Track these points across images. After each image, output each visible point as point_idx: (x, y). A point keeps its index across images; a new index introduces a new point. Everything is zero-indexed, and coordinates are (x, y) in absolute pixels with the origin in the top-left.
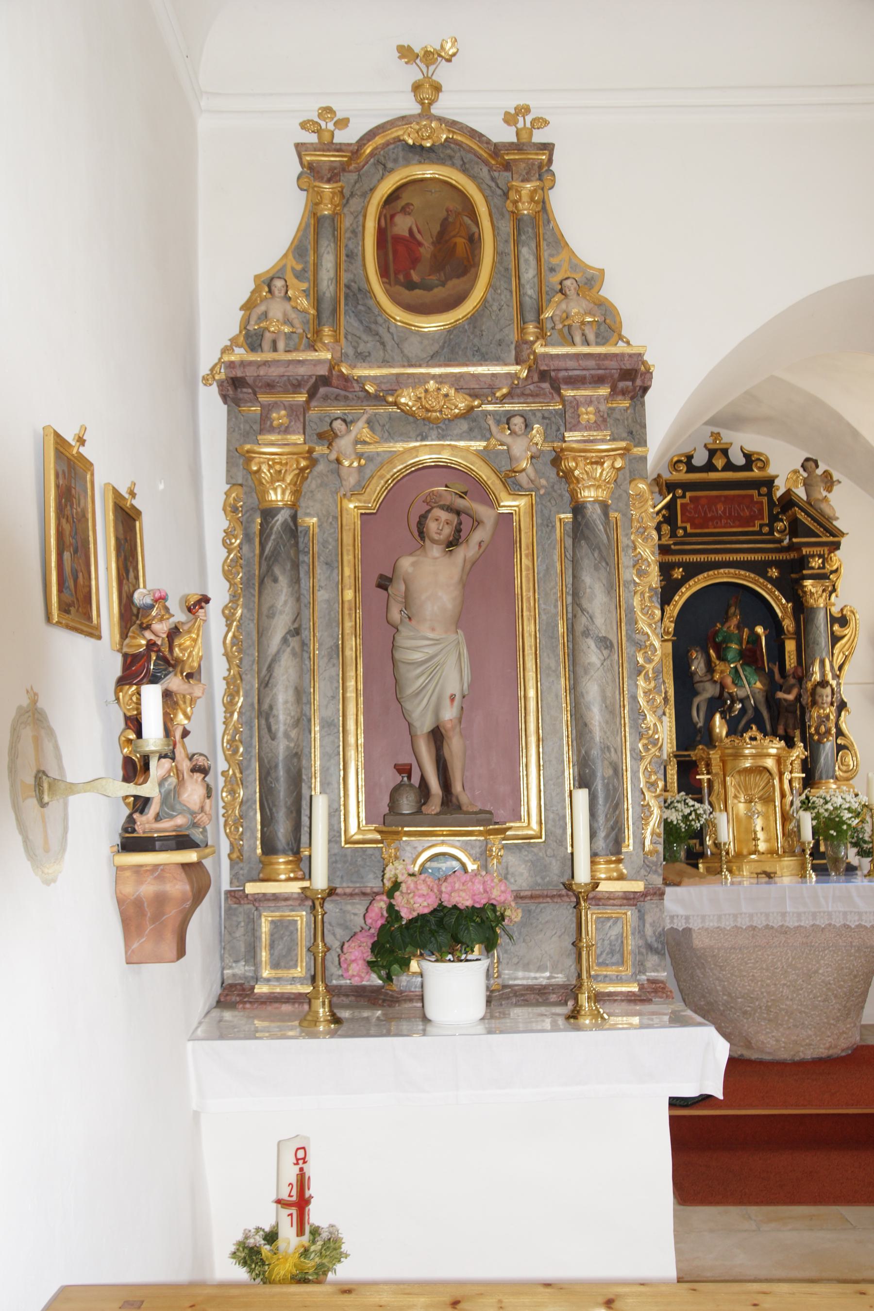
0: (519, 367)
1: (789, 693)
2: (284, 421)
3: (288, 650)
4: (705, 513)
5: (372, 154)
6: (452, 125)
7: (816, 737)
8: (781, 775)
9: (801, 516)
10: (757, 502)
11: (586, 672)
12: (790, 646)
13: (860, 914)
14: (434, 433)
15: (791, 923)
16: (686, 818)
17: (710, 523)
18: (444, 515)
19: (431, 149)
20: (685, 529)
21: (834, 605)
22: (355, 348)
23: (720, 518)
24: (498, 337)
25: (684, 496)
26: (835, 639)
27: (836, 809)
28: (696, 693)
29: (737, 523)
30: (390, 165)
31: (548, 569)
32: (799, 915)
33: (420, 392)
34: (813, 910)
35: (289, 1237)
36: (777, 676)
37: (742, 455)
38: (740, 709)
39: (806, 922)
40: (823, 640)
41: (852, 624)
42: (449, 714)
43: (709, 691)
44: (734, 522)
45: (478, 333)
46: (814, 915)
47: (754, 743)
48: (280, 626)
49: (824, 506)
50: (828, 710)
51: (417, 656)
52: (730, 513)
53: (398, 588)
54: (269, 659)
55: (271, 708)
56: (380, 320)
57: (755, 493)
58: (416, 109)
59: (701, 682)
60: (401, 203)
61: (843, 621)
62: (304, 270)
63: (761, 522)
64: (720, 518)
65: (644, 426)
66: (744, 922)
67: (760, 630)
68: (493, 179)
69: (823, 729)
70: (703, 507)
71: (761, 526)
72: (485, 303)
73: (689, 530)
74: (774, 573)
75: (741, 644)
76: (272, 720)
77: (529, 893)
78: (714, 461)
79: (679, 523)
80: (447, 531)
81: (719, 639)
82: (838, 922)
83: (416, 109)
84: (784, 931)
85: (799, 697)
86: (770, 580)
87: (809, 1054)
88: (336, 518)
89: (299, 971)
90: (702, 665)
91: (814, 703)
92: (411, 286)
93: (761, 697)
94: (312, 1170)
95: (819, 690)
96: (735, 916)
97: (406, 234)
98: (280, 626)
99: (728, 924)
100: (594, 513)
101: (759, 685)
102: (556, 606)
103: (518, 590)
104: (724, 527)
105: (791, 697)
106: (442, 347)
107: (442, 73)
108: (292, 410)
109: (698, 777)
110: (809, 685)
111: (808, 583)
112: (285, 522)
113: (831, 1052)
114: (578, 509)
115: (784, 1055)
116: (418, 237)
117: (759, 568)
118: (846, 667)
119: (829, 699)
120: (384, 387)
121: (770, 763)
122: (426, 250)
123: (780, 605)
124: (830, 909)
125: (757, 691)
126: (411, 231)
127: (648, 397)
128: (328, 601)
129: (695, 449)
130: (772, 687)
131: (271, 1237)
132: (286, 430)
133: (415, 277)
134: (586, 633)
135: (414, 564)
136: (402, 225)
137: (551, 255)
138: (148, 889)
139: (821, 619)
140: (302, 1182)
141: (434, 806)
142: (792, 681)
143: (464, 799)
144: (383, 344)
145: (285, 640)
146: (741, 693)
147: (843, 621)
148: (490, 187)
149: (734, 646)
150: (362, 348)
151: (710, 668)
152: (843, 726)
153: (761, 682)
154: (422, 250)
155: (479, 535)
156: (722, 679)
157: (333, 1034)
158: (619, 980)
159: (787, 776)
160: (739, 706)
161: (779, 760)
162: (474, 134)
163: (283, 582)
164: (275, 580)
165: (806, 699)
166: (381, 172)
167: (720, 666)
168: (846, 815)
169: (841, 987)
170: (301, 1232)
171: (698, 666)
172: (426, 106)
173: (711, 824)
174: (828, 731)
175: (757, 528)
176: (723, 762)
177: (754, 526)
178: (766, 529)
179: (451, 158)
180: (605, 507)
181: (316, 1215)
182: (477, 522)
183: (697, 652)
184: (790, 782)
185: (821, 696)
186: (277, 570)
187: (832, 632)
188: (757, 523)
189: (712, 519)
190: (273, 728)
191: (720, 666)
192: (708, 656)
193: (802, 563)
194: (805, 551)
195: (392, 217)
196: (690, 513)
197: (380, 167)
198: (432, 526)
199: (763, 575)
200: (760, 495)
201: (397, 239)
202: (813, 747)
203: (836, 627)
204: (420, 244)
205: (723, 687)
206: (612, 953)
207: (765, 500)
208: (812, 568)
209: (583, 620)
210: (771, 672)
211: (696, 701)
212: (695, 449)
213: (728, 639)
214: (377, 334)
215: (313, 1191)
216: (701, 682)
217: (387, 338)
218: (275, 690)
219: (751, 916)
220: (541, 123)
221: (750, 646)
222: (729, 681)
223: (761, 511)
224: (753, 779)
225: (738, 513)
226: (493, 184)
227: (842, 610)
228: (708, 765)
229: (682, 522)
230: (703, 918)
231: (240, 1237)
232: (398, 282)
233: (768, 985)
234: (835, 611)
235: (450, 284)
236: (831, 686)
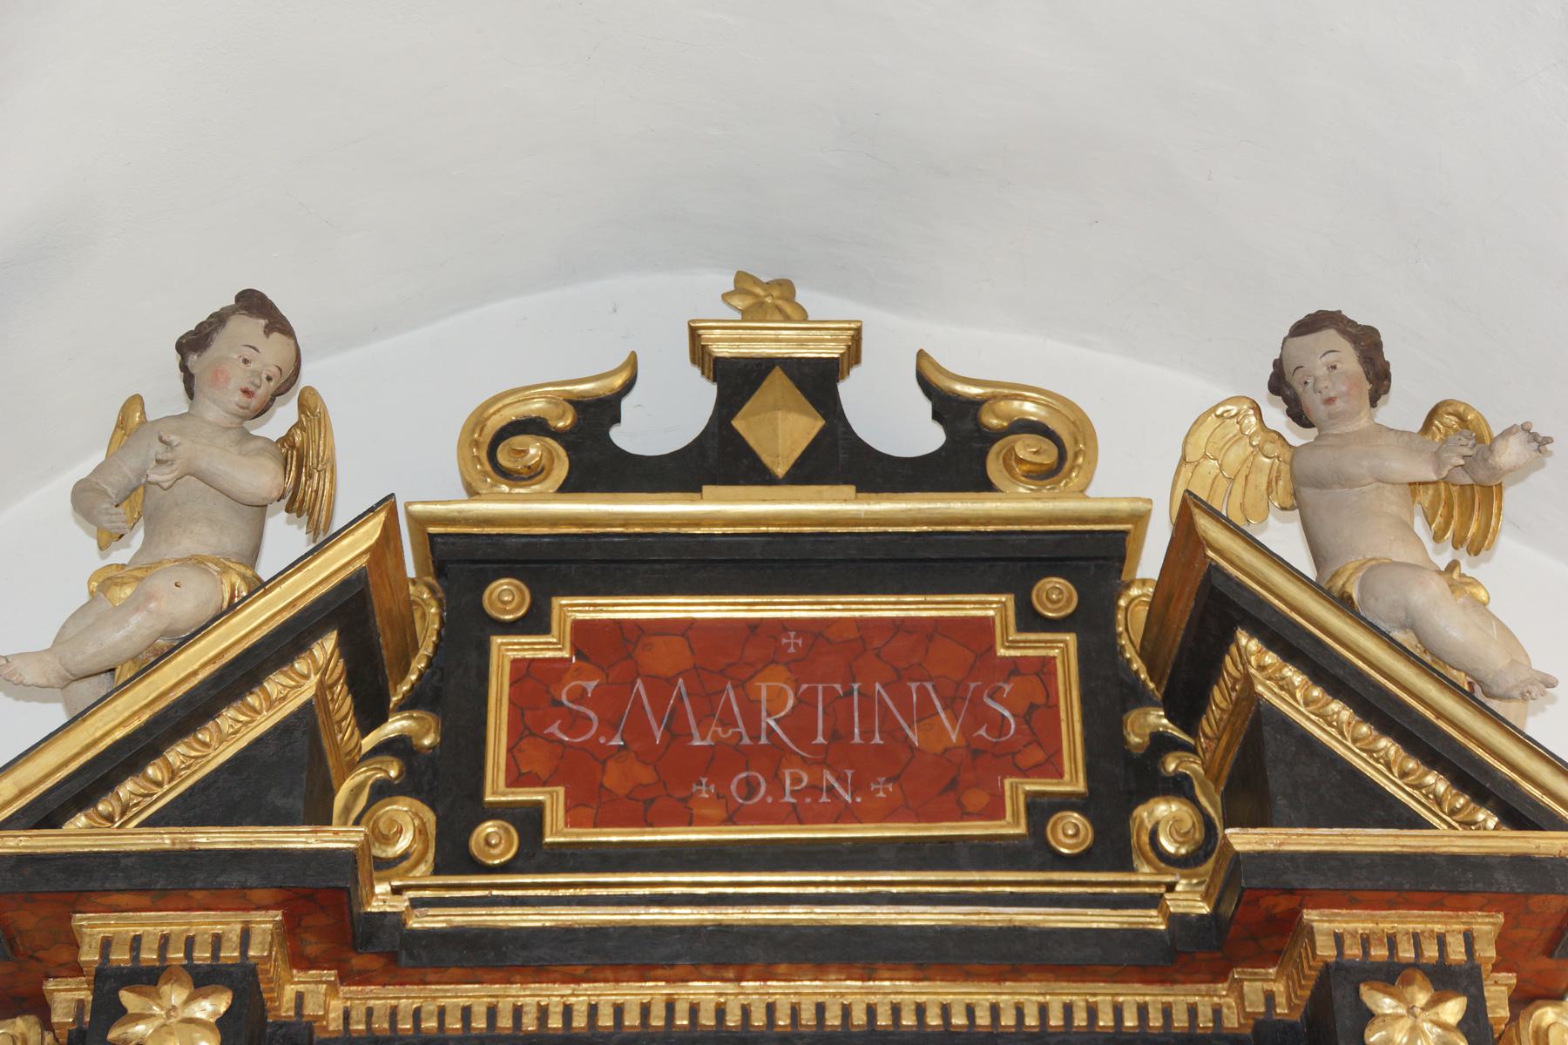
4: (677, 731)
10: (1014, 667)
17: (705, 790)
20: (528, 820)
23: (774, 757)
25: (535, 621)
29: (882, 790)
37: (926, 406)
44: (858, 787)
52: (838, 734)
57: (992, 606)
64: (774, 757)
70: (660, 687)
71: (1041, 810)
73: (557, 832)
78: (738, 423)
79: (496, 790)
104: (797, 816)
129: (632, 362)
175: (1012, 826)
177: (994, 811)
178: (1070, 833)
188: (1017, 789)
189: (719, 761)
196: (575, 723)
200: (1030, 619)
207: (1063, 648)
212: (632, 362)
223: (1039, 718)
225: (893, 732)
229: (516, 778)
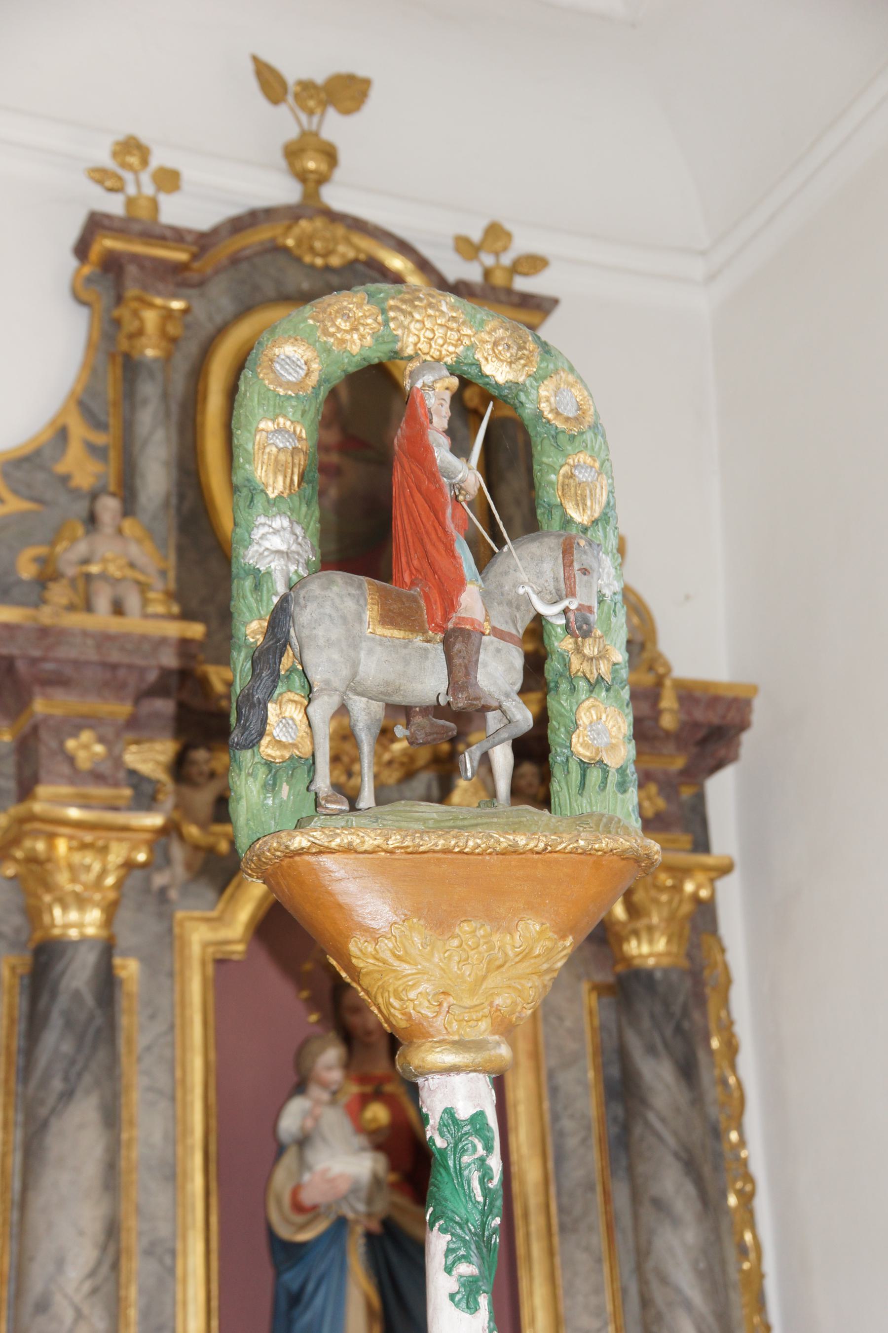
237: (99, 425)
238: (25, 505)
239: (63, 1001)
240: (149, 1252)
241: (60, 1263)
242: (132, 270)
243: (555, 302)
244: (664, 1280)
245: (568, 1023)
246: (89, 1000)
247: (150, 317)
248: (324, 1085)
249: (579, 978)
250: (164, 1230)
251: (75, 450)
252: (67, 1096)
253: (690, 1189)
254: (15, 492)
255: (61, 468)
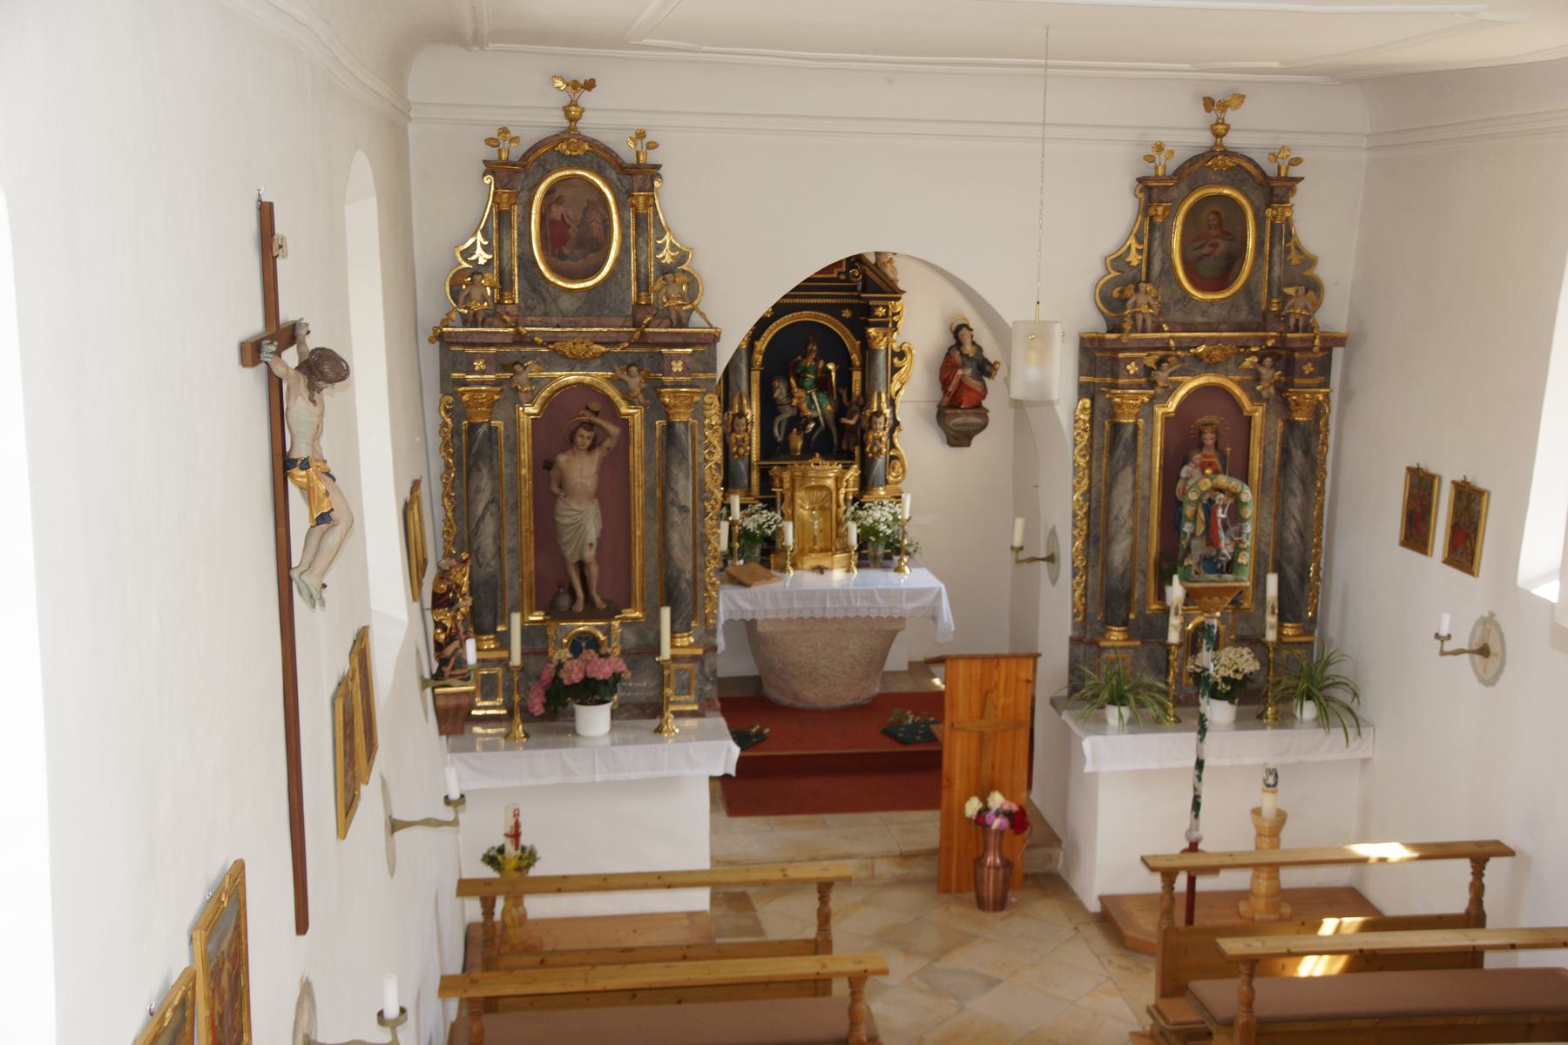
0: (635, 329)
1: (851, 418)
2: (483, 367)
3: (489, 513)
5: (535, 160)
6: (592, 142)
7: (870, 455)
8: (838, 489)
9: (869, 273)
11: (672, 526)
12: (857, 376)
13: (879, 609)
14: (578, 366)
15: (829, 615)
16: (760, 527)
18: (586, 434)
19: (578, 156)
21: (894, 341)
22: (525, 302)
24: (621, 297)
26: (895, 370)
27: (875, 521)
28: (779, 413)
30: (548, 167)
31: (650, 455)
32: (835, 609)
33: (570, 344)
34: (845, 605)
35: (510, 850)
36: (845, 400)
38: (814, 428)
39: (841, 615)
40: (881, 376)
41: (909, 356)
42: (589, 554)
43: (788, 413)
45: (608, 293)
46: (846, 609)
47: (817, 467)
48: (484, 497)
49: (888, 271)
50: (881, 434)
51: (566, 521)
53: (554, 474)
54: (477, 519)
55: (478, 548)
56: (542, 282)
58: (565, 123)
59: (781, 405)
60: (556, 195)
61: (901, 355)
62: (490, 244)
63: (840, 270)
65: (715, 359)
66: (795, 615)
67: (831, 366)
68: (620, 180)
69: (875, 449)
71: (839, 273)
72: (612, 273)
74: (847, 314)
75: (816, 373)
76: (479, 556)
77: (635, 651)
80: (588, 442)
81: (799, 371)
82: (863, 614)
83: (565, 123)
84: (824, 620)
85: (859, 421)
86: (843, 321)
87: (838, 703)
88: (513, 422)
89: (499, 701)
90: (784, 391)
91: (870, 428)
92: (563, 257)
93: (830, 418)
94: (521, 819)
95: (874, 418)
96: (789, 611)
97: (559, 219)
98: (484, 497)
99: (783, 616)
100: (680, 429)
101: (829, 407)
102: (655, 478)
103: (631, 469)
105: (852, 422)
106: (584, 303)
107: (586, 99)
108: (488, 359)
109: (773, 490)
110: (868, 413)
111: (872, 331)
112: (484, 434)
113: (856, 701)
114: (670, 427)
115: (821, 705)
116: (568, 221)
117: (834, 311)
118: (901, 393)
119: (882, 426)
120: (546, 340)
121: (830, 483)
122: (573, 232)
123: (851, 343)
124: (858, 605)
125: (827, 412)
126: (562, 217)
127: (718, 344)
128: (511, 475)
130: (841, 411)
131: (501, 850)
132: (482, 372)
133: (566, 251)
134: (673, 503)
135: (567, 461)
136: (557, 212)
137: (659, 239)
138: (452, 702)
139: (881, 357)
140: (517, 825)
141: (580, 606)
142: (855, 408)
143: (598, 600)
144: (544, 300)
145: (486, 508)
146: (815, 415)
147: (901, 355)
148: (617, 186)
149: (812, 377)
150: (530, 302)
151: (790, 395)
152: (896, 441)
153: (831, 405)
154: (570, 230)
155: (608, 443)
156: (799, 404)
157: (526, 747)
158: (687, 703)
159: (843, 491)
160: (812, 425)
161: (838, 480)
162: (606, 150)
163: (485, 470)
164: (479, 470)
165: (865, 424)
166: (542, 172)
167: (798, 392)
168: (883, 527)
169: (864, 658)
170: (517, 848)
171: (780, 392)
172: (573, 120)
173: (780, 532)
174: (880, 451)
175: (835, 275)
176: (793, 480)
179: (591, 162)
180: (686, 423)
181: (525, 840)
182: (607, 435)
183: (779, 382)
184: (846, 494)
185: (876, 423)
186: (480, 464)
187: (892, 364)
190: (481, 560)
191: (798, 392)
192: (789, 383)
193: (868, 310)
194: (871, 303)
195: (550, 205)
197: (541, 169)
198: (579, 440)
199: (838, 316)
201: (553, 222)
202: (866, 466)
203: (896, 360)
204: (569, 227)
205: (799, 410)
206: (683, 688)
208: (877, 317)
209: (671, 495)
210: (840, 396)
211: (778, 419)
213: (806, 370)
214: (540, 293)
215: (523, 829)
216: (781, 405)
217: (547, 295)
218: (481, 538)
219: (801, 610)
220: (652, 146)
221: (823, 375)
222: (804, 406)
224: (817, 494)
226: (618, 184)
227: (901, 347)
228: (781, 481)
230: (766, 612)
231: (485, 851)
232: (554, 255)
233: (811, 658)
234: (895, 346)
235: (590, 256)
236: (885, 415)
237: (1141, 243)
238: (1118, 274)
239: (1123, 440)
240: (1143, 498)
241: (1121, 508)
242: (1155, 190)
243: (1303, 178)
244: (1289, 510)
245: (1272, 432)
246: (1130, 439)
247: (1160, 209)
248: (1194, 463)
249: (1278, 418)
250: (1147, 492)
251: (1133, 251)
252: (1124, 466)
253: (1301, 487)
254: (1114, 269)
255: (1128, 260)
